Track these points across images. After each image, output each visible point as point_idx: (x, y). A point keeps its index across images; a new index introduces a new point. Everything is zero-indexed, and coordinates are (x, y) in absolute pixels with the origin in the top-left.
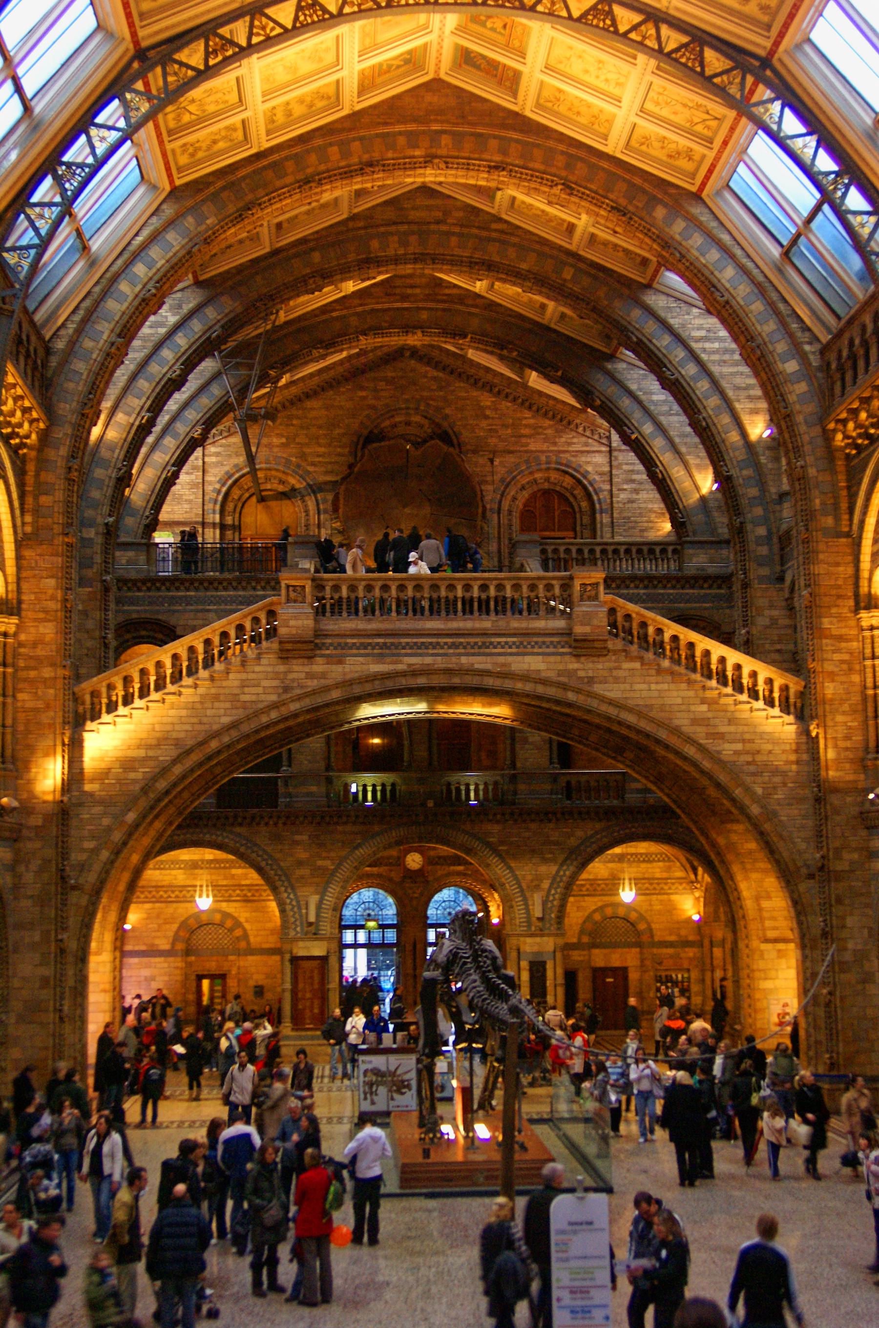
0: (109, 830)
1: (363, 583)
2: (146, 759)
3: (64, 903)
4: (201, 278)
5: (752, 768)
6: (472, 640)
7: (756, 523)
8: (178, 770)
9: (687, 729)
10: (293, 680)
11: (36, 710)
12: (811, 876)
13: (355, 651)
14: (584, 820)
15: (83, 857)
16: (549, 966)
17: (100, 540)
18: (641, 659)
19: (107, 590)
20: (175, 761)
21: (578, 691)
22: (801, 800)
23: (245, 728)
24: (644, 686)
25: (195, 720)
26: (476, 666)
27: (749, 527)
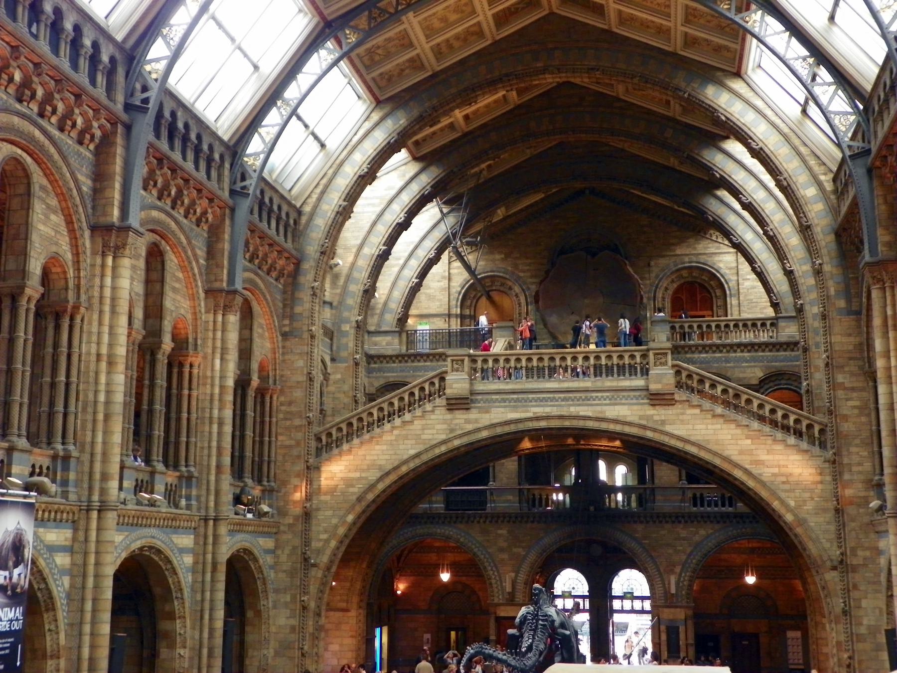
0: (336, 527)
1: (503, 358)
3: (306, 575)
4: (418, 156)
5: (787, 487)
6: (578, 395)
7: (812, 304)
8: (381, 486)
9: (736, 458)
10: (456, 425)
11: (290, 447)
12: (834, 568)
14: (705, 522)
15: (321, 544)
16: (682, 629)
17: (353, 331)
18: (700, 406)
19: (357, 364)
21: (655, 430)
22: (825, 510)
23: (425, 458)
24: (704, 427)
25: (391, 452)
26: (582, 413)
27: (807, 307)
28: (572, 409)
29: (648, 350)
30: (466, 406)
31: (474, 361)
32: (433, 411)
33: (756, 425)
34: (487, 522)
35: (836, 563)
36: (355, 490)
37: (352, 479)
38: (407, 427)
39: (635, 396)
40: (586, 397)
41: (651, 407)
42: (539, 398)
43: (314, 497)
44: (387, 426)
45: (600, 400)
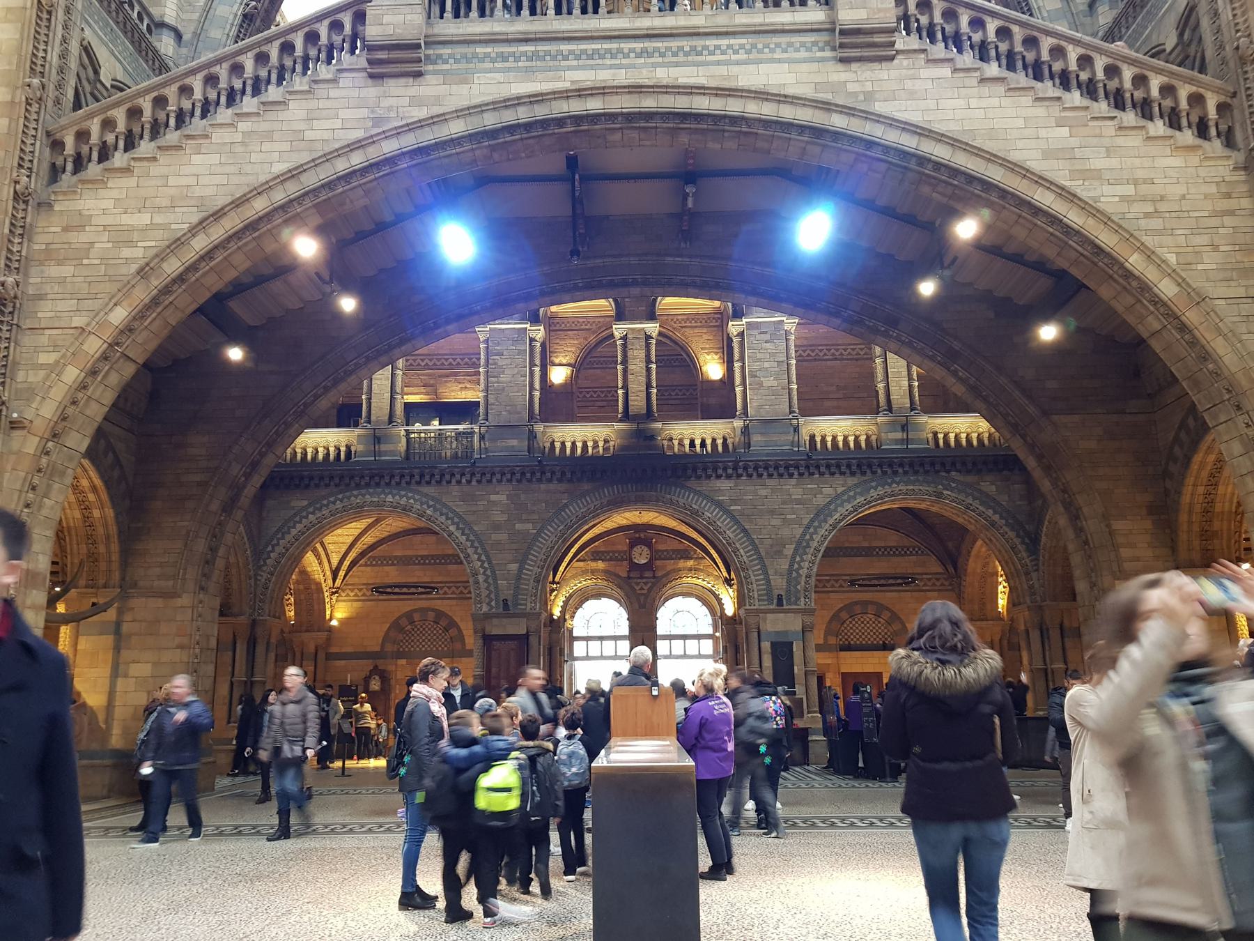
2: (152, 226)
5: (1156, 224)
6: (674, 44)
8: (200, 244)
9: (1036, 166)
10: (390, 108)
13: (488, 65)
15: (35, 377)
20: (194, 230)
21: (849, 111)
25: (232, 169)
26: (681, 81)
28: (664, 75)
30: (414, 68)
34: (474, 483)
36: (138, 253)
37: (131, 229)
38: (271, 115)
39: (803, 45)
40: (693, 48)
41: (840, 67)
42: (584, 52)
43: (33, 271)
44: (224, 114)
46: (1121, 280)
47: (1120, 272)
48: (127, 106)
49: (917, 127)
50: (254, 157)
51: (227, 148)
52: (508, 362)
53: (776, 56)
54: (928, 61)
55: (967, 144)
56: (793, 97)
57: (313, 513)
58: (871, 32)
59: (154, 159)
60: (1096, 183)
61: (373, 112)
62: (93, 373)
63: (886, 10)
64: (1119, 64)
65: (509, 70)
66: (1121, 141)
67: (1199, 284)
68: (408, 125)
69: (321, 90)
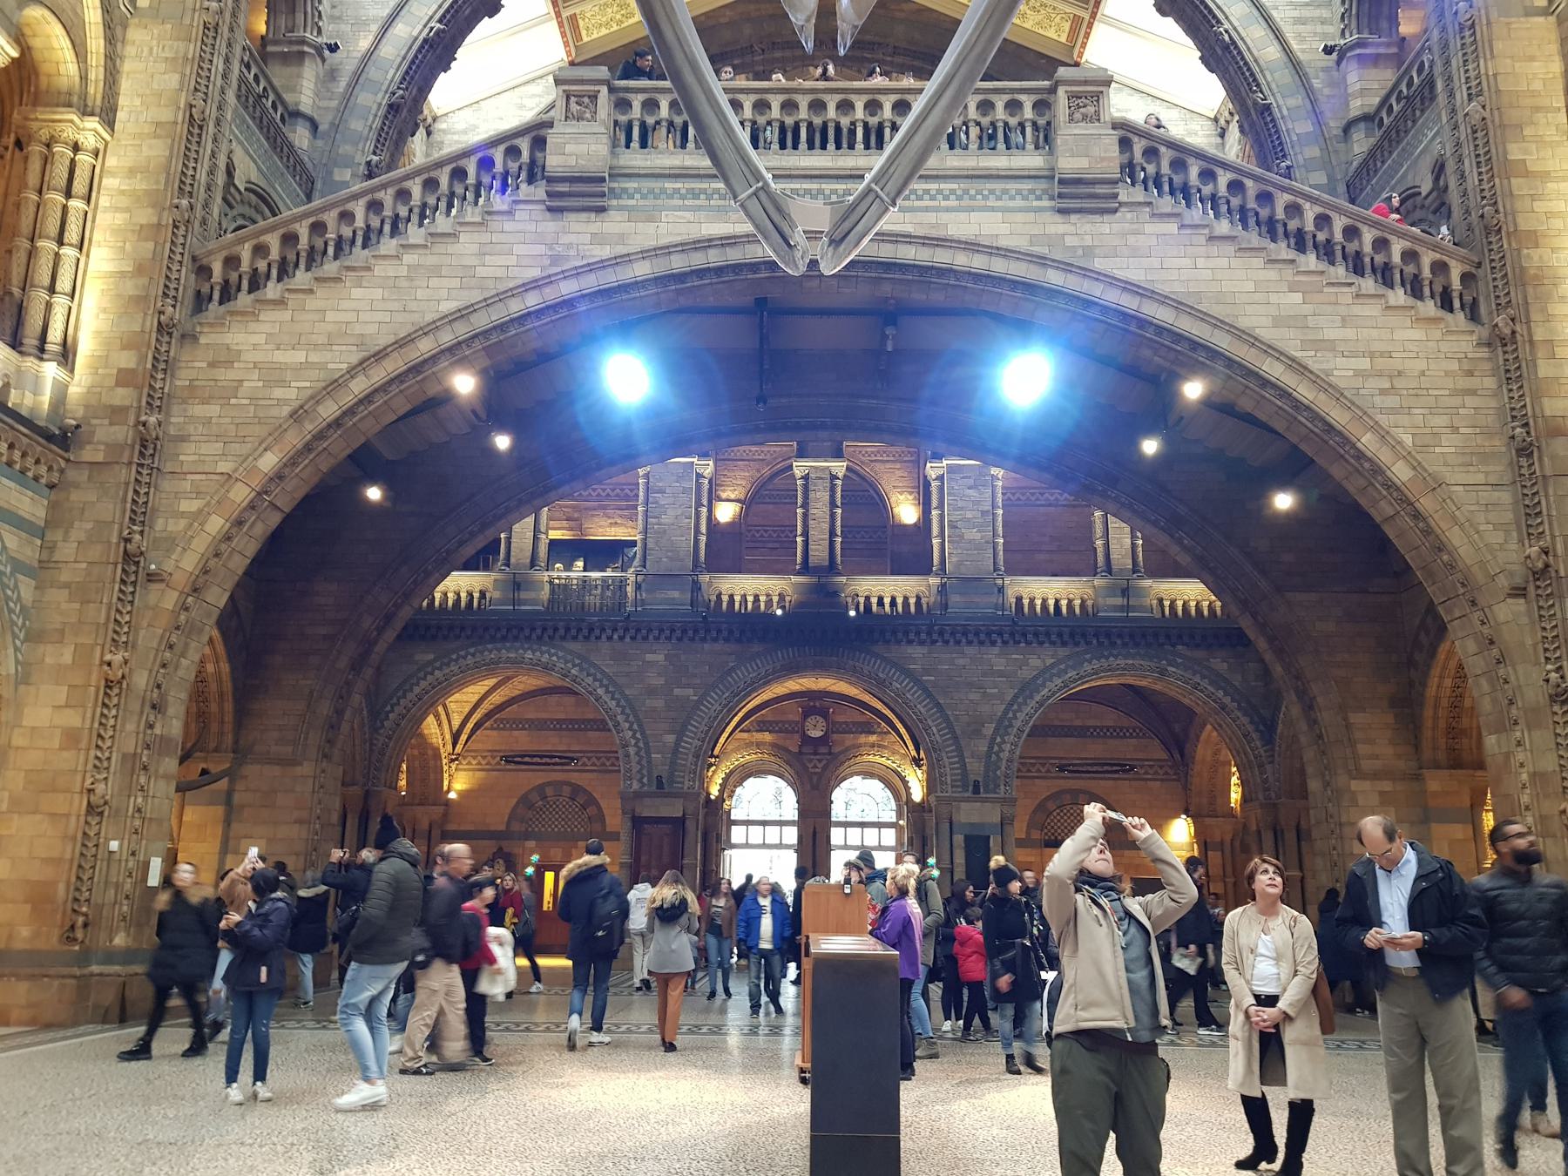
2: (307, 365)
5: (1391, 401)
8: (359, 386)
9: (1267, 334)
12: (1519, 592)
15: (177, 526)
20: (352, 372)
21: (1066, 267)
22: (1485, 458)
24: (1187, 262)
25: (396, 306)
29: (1053, 90)
30: (598, 202)
31: (623, 105)
32: (510, 213)
33: (1310, 260)
34: (627, 639)
35: (1519, 581)
36: (291, 394)
37: (283, 367)
38: (439, 248)
39: (1019, 192)
41: (1058, 218)
43: (175, 409)
44: (388, 245)
45: (933, 198)
46: (1352, 461)
47: (1352, 451)
48: (282, 231)
49: (1139, 287)
50: (420, 294)
51: (391, 283)
52: (671, 500)
53: (989, 204)
54: (1153, 215)
55: (1192, 308)
56: (1006, 250)
57: (440, 669)
58: (1093, 182)
59: (311, 291)
60: (1329, 355)
61: (551, 249)
62: (239, 523)
63: (1110, 159)
64: (1360, 225)
65: (699, 208)
66: (1358, 310)
67: (1435, 468)
68: (589, 265)
69: (496, 223)
